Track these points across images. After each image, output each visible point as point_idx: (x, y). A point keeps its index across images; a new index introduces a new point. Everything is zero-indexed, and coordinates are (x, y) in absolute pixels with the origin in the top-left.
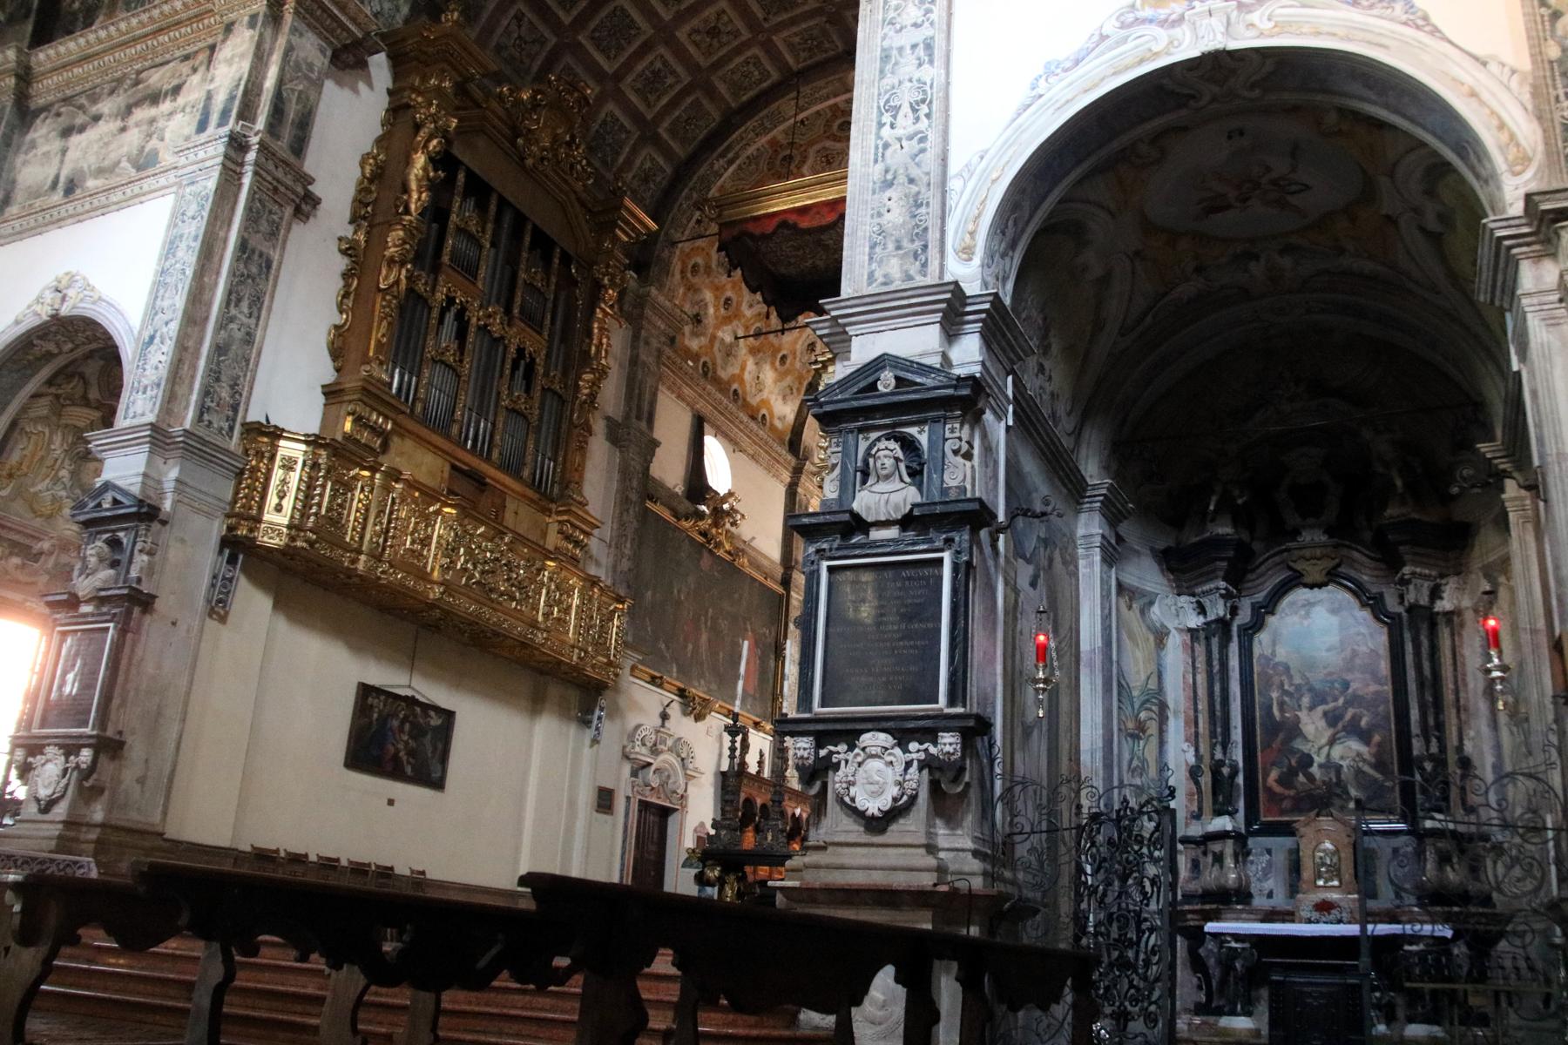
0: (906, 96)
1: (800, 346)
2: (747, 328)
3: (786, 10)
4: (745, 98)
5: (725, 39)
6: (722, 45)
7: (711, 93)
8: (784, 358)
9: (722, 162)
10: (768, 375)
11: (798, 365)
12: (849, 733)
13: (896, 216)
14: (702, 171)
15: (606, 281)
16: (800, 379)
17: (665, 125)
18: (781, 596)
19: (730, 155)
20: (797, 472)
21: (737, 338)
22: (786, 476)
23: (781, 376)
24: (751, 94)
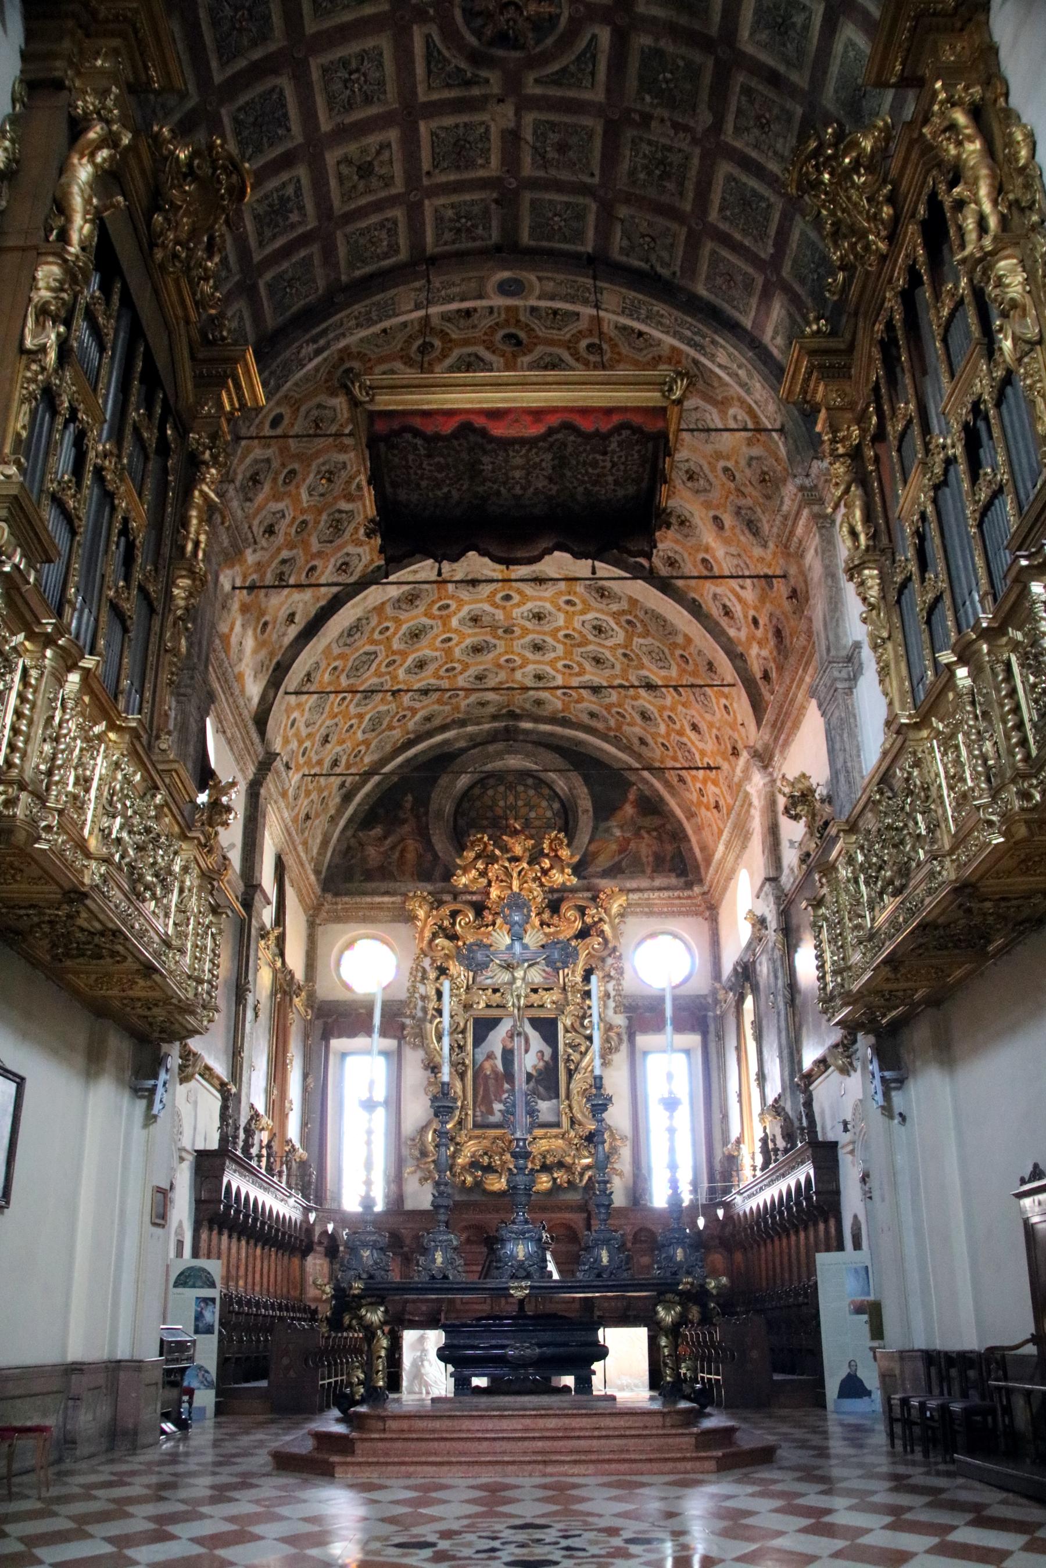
1: (283, 614)
2: (245, 577)
3: (458, 168)
4: (358, 273)
5: (375, 182)
6: (369, 191)
7: (329, 253)
8: (266, 624)
9: (312, 347)
10: (249, 643)
11: (274, 636)
14: (287, 354)
15: (207, 455)
16: (272, 654)
17: (269, 276)
18: (243, 921)
19: (322, 342)
20: (265, 765)
21: (234, 588)
22: (251, 770)
23: (260, 645)
24: (368, 269)
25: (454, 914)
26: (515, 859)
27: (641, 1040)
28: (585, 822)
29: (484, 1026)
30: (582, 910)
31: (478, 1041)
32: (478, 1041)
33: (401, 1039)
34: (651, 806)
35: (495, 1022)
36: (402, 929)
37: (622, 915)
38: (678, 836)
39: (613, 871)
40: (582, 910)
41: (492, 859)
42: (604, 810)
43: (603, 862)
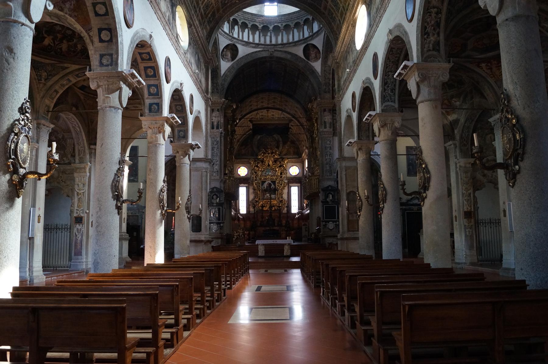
0: (328, 154)
12: (328, 222)
13: (328, 168)
25: (258, 163)
26: (269, 154)
27: (290, 185)
28: (281, 145)
29: (263, 182)
30: (280, 162)
31: (262, 185)
32: (262, 185)
33: (249, 184)
34: (293, 142)
35: (265, 182)
36: (248, 165)
37: (287, 163)
38: (298, 148)
39: (286, 155)
40: (280, 162)
41: (264, 153)
42: (285, 143)
43: (284, 153)
